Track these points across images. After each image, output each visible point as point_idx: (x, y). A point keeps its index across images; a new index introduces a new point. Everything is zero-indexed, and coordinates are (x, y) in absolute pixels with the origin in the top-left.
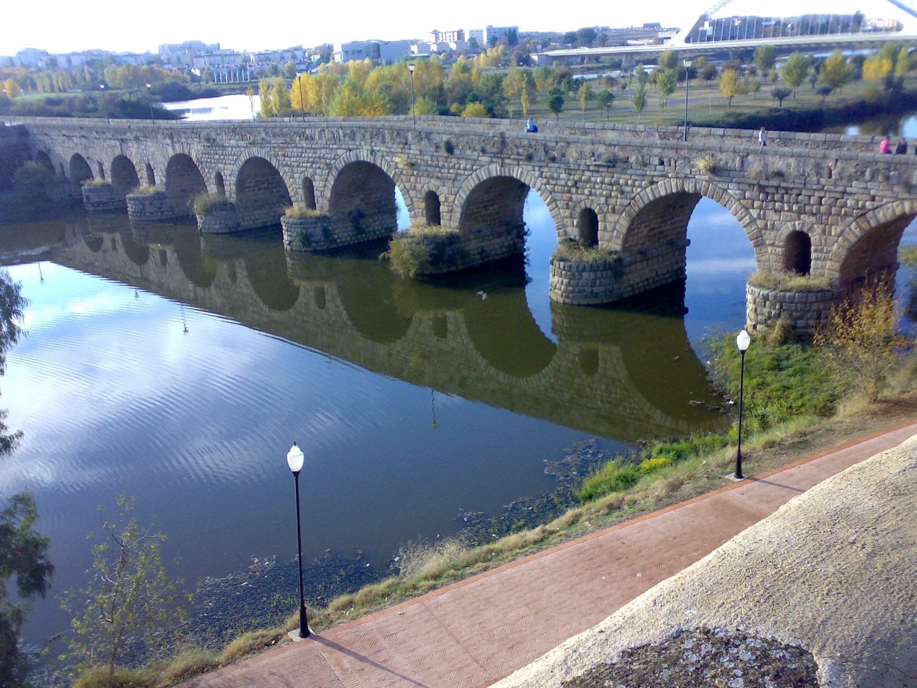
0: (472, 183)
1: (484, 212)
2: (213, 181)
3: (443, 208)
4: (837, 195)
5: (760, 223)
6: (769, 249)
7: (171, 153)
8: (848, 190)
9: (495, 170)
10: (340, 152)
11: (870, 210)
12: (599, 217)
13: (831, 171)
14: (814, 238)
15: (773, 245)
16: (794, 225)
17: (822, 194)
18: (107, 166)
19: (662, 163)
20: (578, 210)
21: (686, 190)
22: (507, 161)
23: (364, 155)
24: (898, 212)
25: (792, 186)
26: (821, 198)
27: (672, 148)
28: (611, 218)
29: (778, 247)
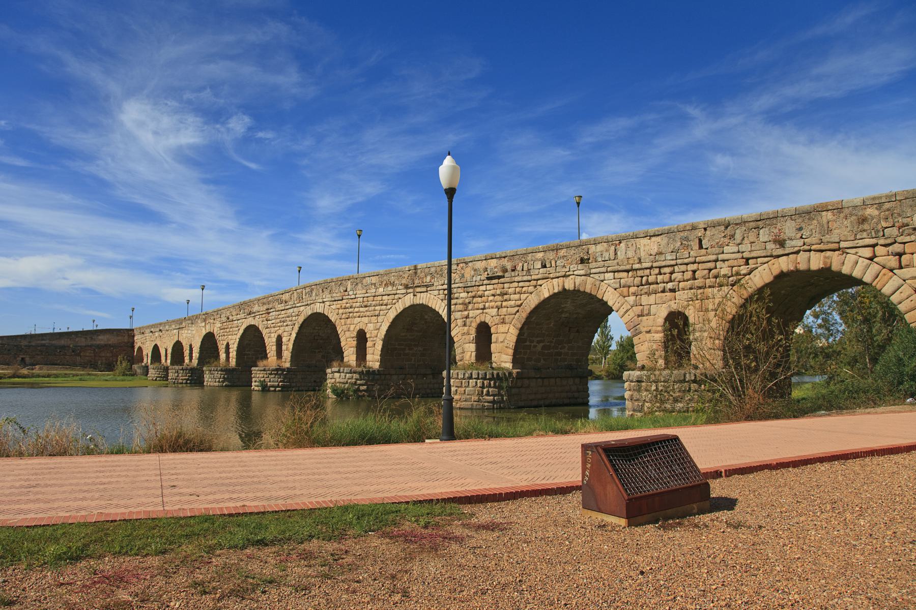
0: (392, 315)
1: (407, 351)
2: (224, 350)
3: (369, 344)
4: (711, 265)
5: (638, 310)
6: (648, 335)
7: (204, 332)
8: (721, 257)
9: (409, 300)
10: (302, 308)
11: (745, 275)
12: (493, 330)
13: (700, 241)
14: (691, 314)
15: (649, 332)
16: (669, 306)
17: (695, 267)
18: (170, 351)
19: (544, 266)
20: (474, 325)
21: (567, 287)
22: (418, 290)
23: (318, 308)
24: (776, 272)
25: (664, 264)
26: (694, 272)
27: (553, 250)
28: (502, 328)
29: (657, 332)
